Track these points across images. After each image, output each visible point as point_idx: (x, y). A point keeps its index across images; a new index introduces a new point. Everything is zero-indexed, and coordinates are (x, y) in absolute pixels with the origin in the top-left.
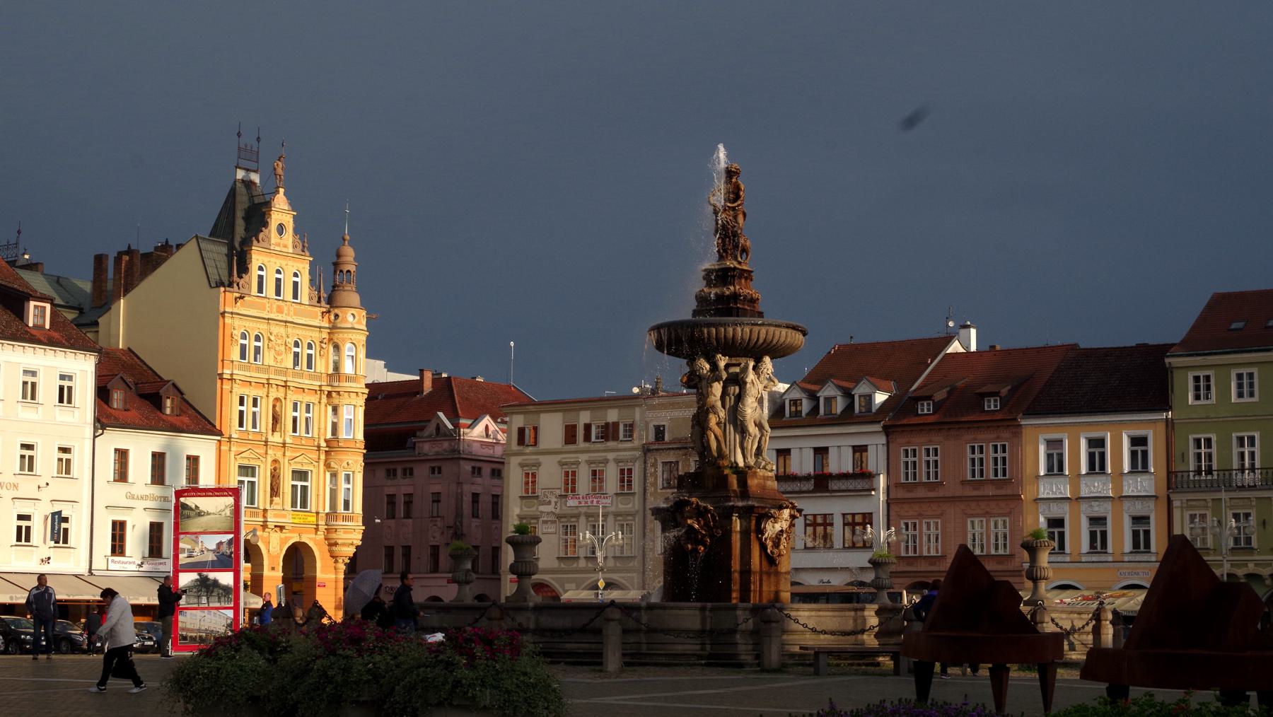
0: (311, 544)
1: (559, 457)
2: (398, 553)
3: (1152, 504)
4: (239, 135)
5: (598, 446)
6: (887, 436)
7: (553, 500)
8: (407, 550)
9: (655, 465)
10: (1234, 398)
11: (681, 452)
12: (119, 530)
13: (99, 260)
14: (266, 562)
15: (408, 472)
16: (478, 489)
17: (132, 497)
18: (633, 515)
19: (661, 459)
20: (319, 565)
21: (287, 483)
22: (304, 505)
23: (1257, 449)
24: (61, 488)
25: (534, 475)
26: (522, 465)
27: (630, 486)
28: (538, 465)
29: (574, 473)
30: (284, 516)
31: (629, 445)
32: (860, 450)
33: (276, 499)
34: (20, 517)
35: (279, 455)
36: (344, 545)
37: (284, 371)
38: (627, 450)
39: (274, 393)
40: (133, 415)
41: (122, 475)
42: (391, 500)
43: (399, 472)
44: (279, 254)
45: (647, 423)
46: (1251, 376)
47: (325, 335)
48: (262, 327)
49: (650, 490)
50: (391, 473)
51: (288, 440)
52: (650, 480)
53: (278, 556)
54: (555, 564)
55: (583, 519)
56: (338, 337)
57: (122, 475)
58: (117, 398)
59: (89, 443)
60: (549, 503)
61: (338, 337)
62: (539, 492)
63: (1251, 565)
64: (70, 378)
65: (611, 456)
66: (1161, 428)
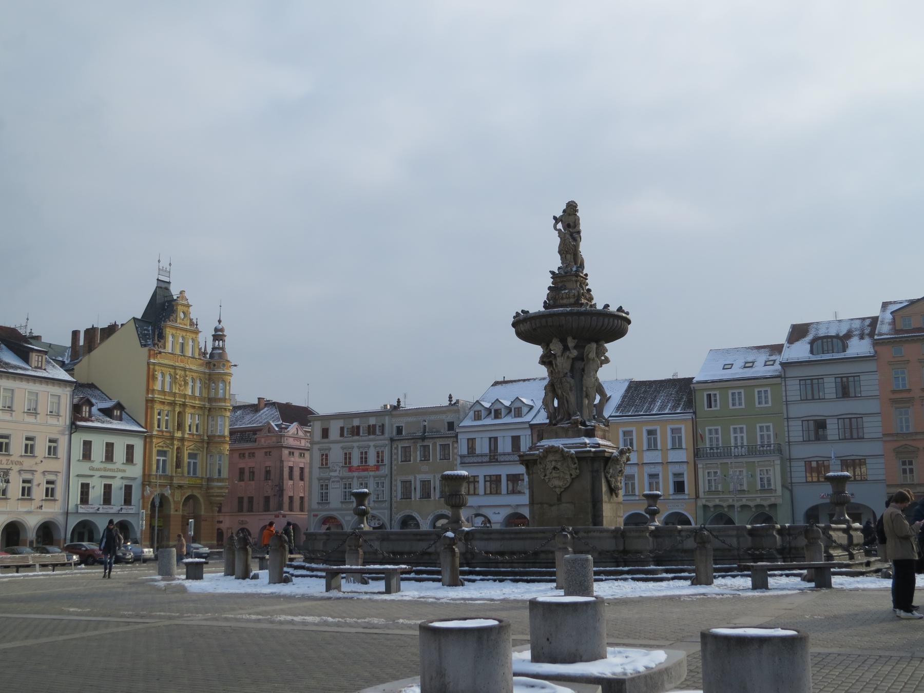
0: (198, 496)
1: (341, 445)
2: (246, 501)
3: (685, 466)
4: (159, 261)
5: (364, 438)
7: (338, 469)
8: (251, 499)
9: (397, 448)
10: (731, 407)
12: (85, 488)
13: (75, 334)
14: (172, 506)
15: (252, 455)
16: (291, 464)
17: (92, 469)
18: (385, 476)
19: (400, 445)
20: (203, 508)
22: (195, 473)
23: (745, 435)
24: (52, 465)
25: (327, 456)
26: (320, 450)
27: (382, 461)
28: (330, 449)
29: (350, 454)
31: (382, 437)
33: (179, 470)
34: (24, 482)
36: (217, 496)
37: (185, 396)
38: (382, 440)
39: (178, 409)
41: (87, 456)
42: (242, 471)
43: (247, 455)
45: (392, 425)
46: (739, 393)
49: (394, 463)
50: (242, 456)
51: (186, 436)
52: (394, 457)
54: (340, 505)
55: (355, 480)
57: (87, 456)
59: (67, 437)
62: (330, 465)
63: (744, 500)
65: (372, 444)
66: (690, 424)
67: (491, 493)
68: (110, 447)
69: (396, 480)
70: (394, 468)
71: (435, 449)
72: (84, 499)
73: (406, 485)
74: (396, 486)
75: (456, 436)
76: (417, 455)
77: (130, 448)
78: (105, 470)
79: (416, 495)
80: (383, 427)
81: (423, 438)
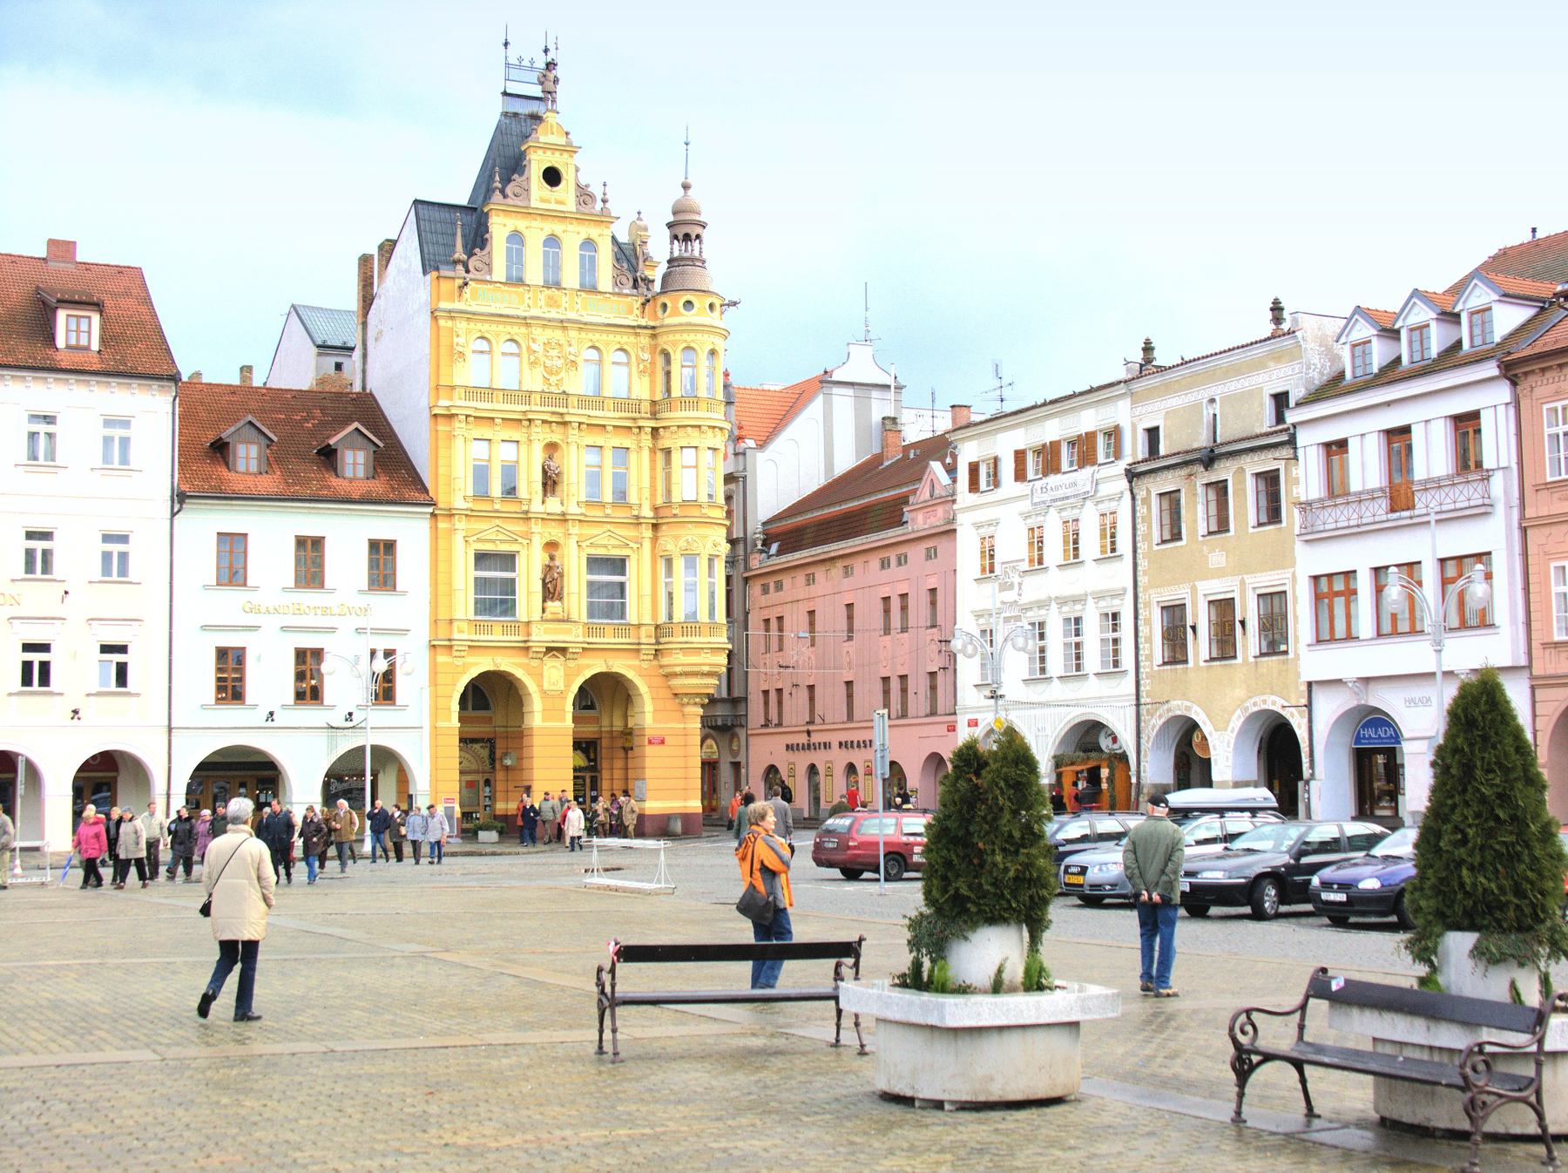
0: (630, 675)
6: (1514, 384)
7: (1016, 579)
9: (1146, 501)
11: (1184, 472)
21: (576, 579)
24: (115, 599)
30: (569, 632)
32: (1466, 424)
33: (553, 606)
34: (27, 647)
35: (555, 532)
36: (686, 674)
39: (542, 435)
40: (269, 483)
43: (893, 561)
44: (546, 215)
47: (645, 340)
48: (518, 331)
53: (562, 694)
56: (664, 341)
58: (247, 455)
60: (1011, 587)
61: (664, 341)
64: (125, 424)
67: (1379, 635)
68: (310, 549)
69: (1147, 605)
70: (1143, 564)
71: (1241, 492)
72: (231, 689)
73: (1175, 615)
74: (1148, 622)
75: (1292, 442)
76: (1197, 514)
77: (382, 551)
78: (298, 612)
79: (1200, 646)
80: (1114, 434)
81: (1209, 459)
